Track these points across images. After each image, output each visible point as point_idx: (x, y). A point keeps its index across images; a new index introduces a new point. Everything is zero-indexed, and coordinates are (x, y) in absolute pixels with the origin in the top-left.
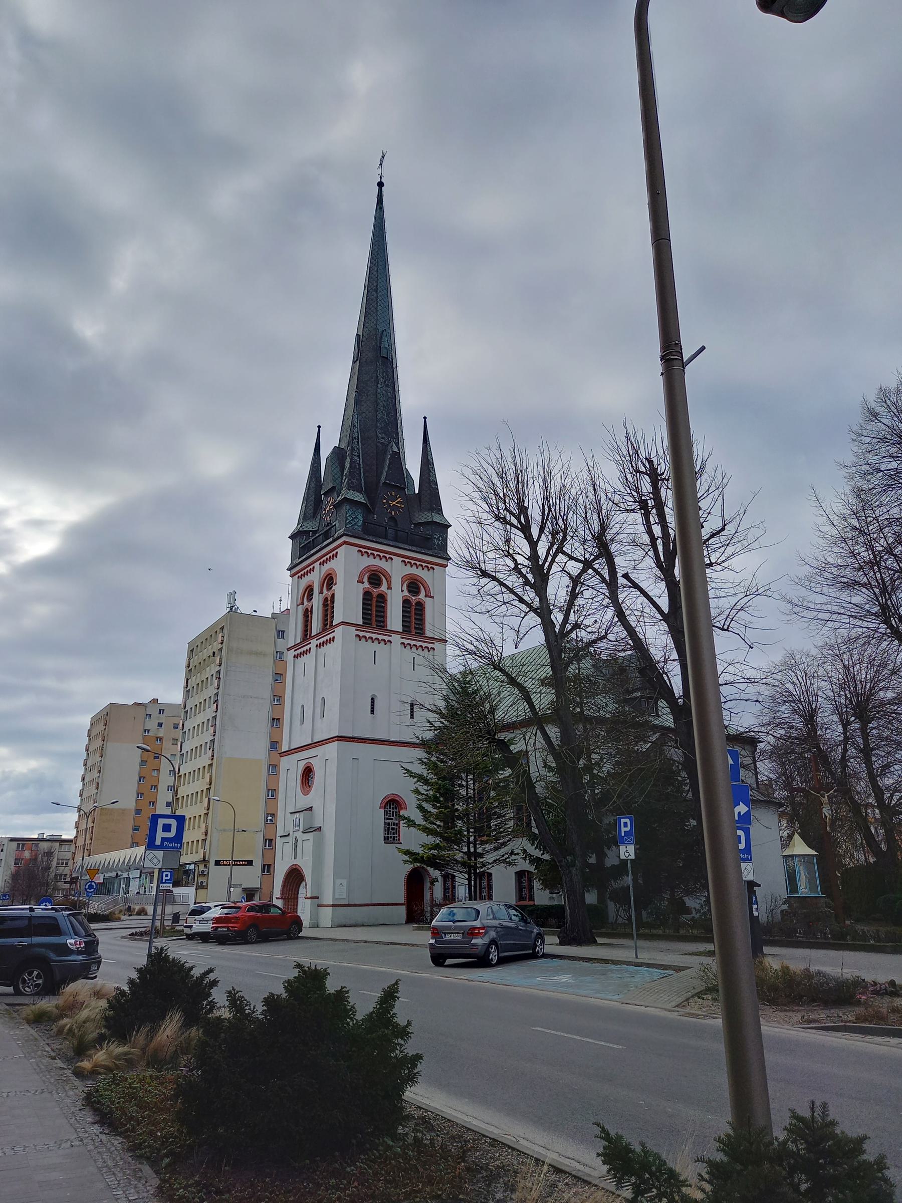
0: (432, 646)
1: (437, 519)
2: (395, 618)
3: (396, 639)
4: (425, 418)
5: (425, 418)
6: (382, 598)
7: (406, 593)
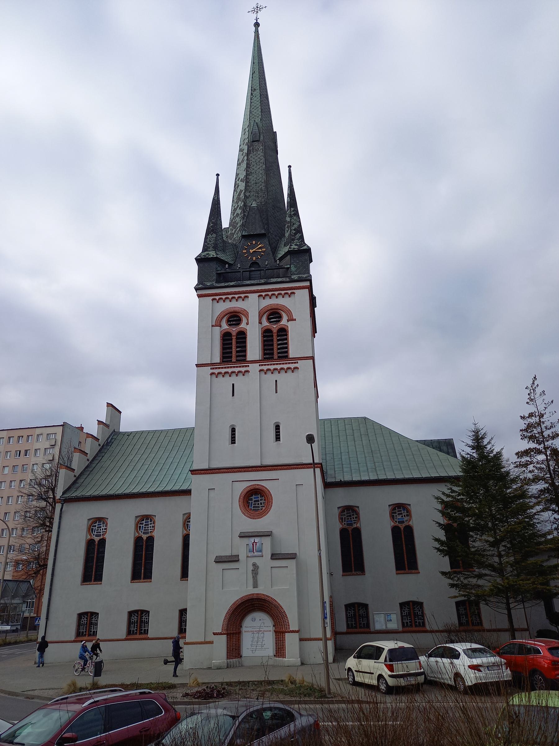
0: (296, 365)
1: (305, 247)
2: (254, 349)
3: (254, 368)
4: (290, 167)
5: (290, 167)
6: (242, 335)
7: (265, 323)
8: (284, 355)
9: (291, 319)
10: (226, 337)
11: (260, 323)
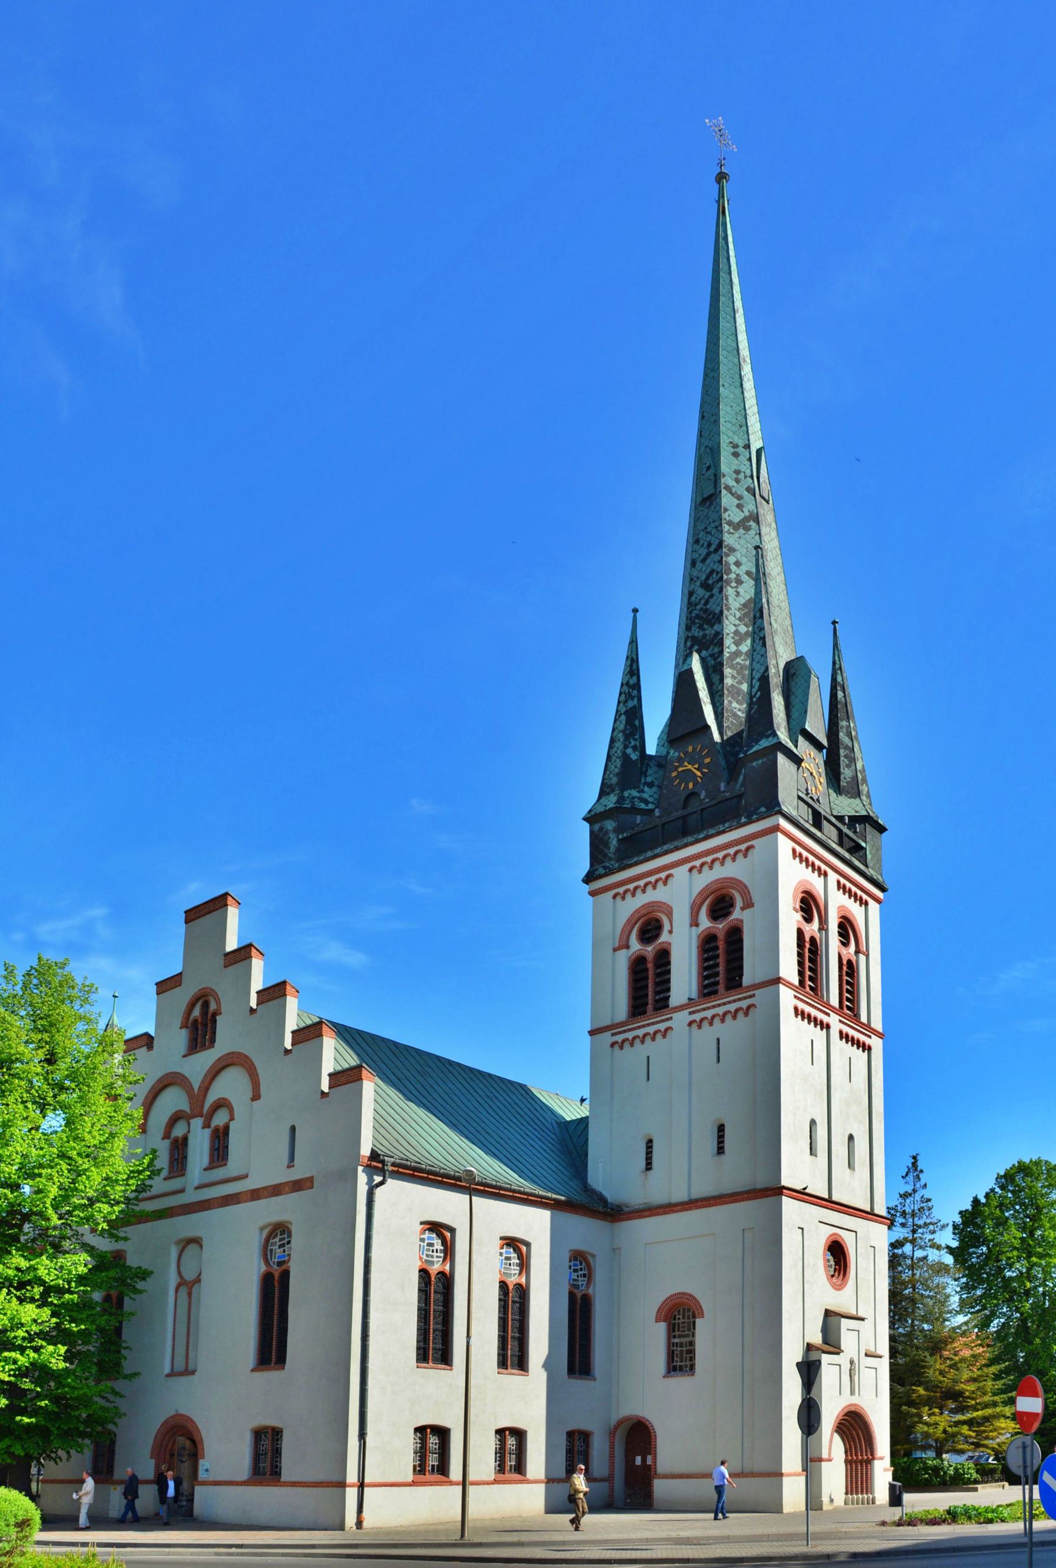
2: (684, 978)
6: (664, 956)
7: (705, 922)
8: (734, 980)
9: (748, 904)
10: (638, 966)
11: (695, 923)
